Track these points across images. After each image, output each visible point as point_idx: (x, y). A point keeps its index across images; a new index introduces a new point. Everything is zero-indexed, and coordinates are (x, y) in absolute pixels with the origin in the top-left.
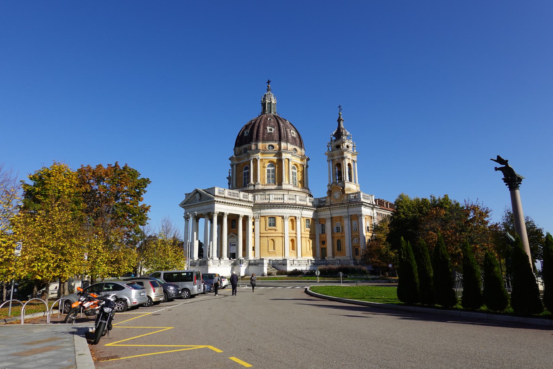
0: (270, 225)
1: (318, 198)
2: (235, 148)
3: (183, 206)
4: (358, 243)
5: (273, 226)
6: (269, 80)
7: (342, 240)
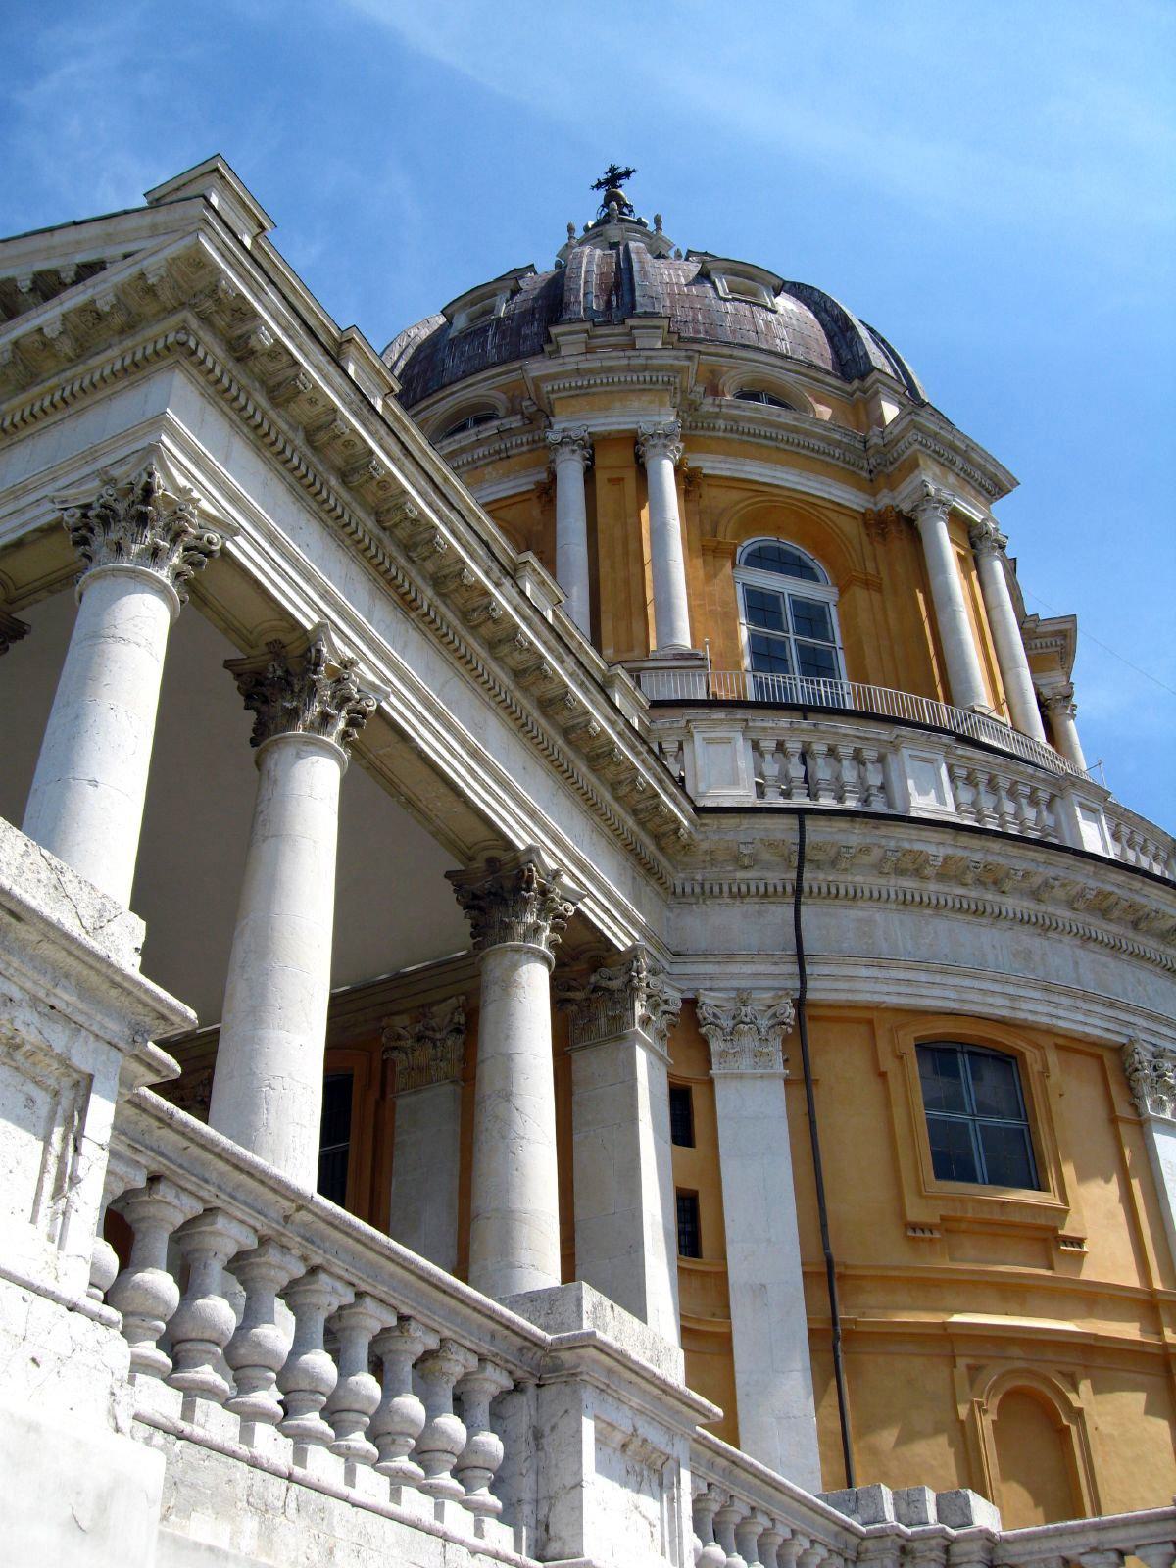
0: (951, 1163)
5: (1001, 1178)
6: (613, 169)
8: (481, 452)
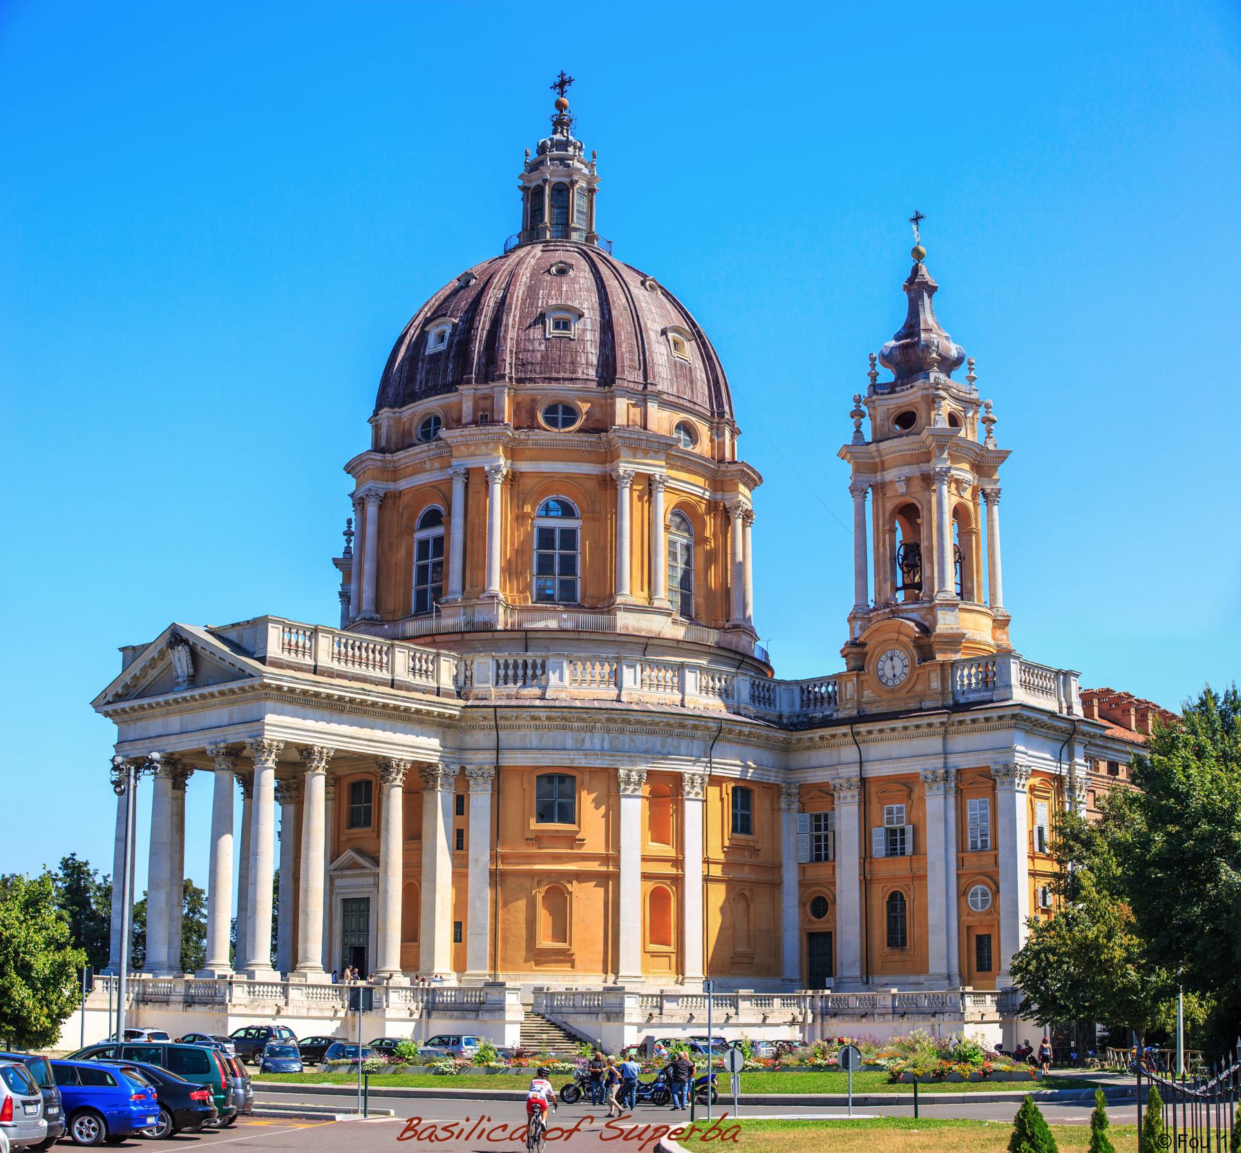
1: (797, 682)
2: (376, 413)
3: (109, 708)
4: (989, 913)
5: (562, 820)
7: (912, 893)
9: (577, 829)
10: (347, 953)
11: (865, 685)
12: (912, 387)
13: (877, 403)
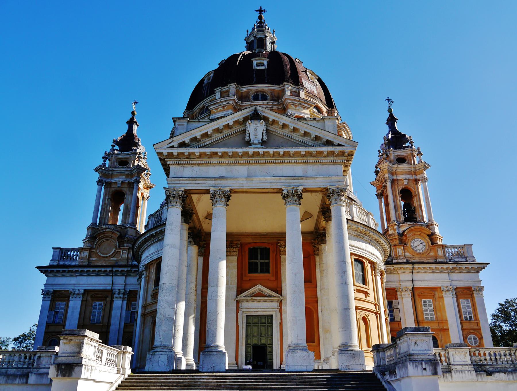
6: (261, 8)
8: (267, 106)
9: (368, 288)
10: (250, 350)
11: (406, 251)
12: (404, 150)
13: (391, 152)
